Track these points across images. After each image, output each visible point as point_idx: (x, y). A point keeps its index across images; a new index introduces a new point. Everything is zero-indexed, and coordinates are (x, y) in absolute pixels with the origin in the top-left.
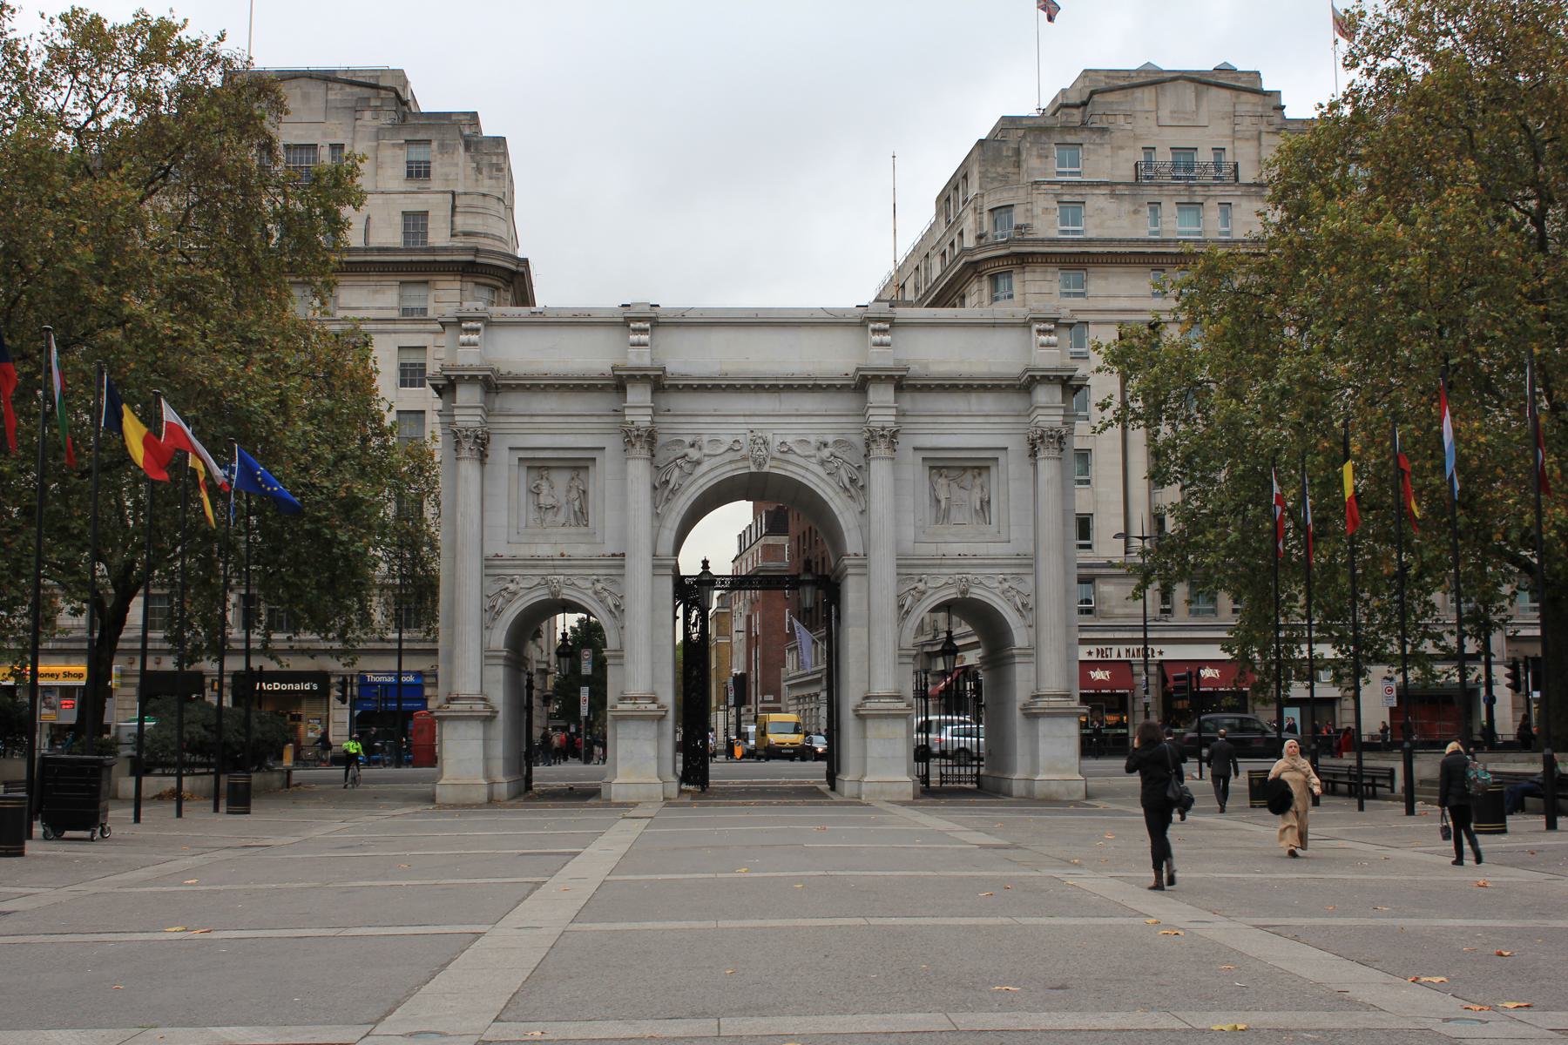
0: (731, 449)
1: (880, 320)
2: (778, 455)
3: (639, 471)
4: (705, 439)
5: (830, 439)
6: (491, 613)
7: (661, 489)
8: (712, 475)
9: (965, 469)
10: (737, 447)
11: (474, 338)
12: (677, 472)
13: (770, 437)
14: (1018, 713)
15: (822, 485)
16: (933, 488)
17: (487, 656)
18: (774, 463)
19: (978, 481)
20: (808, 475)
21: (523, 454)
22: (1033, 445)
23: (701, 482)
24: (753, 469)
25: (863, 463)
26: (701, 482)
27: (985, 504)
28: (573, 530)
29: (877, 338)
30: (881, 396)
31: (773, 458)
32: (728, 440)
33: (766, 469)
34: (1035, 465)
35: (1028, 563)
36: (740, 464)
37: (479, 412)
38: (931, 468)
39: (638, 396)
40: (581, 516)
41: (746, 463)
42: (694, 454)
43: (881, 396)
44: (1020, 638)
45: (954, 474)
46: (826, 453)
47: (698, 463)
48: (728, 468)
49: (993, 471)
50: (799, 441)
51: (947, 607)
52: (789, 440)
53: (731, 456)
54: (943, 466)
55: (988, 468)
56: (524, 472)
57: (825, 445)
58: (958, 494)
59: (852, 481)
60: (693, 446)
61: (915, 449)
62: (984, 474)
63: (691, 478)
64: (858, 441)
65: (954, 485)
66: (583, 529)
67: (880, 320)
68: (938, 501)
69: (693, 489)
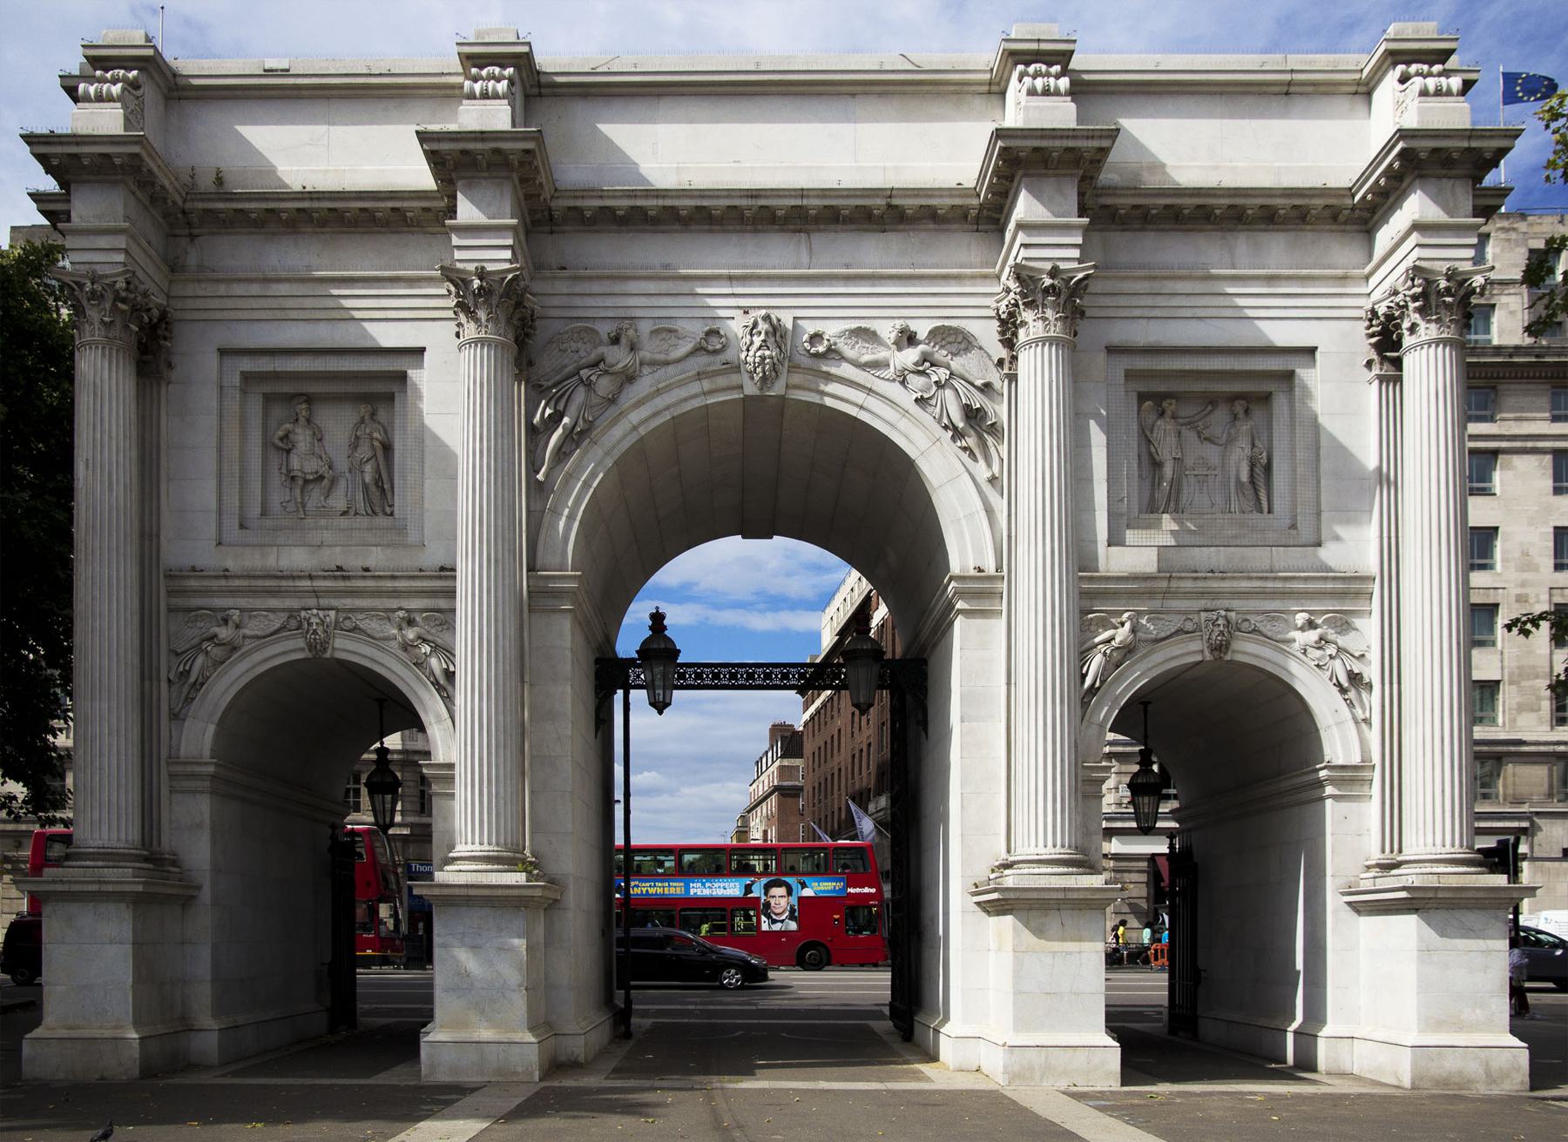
0: (699, 350)
2: (806, 362)
4: (645, 327)
5: (922, 329)
8: (660, 402)
9: (1212, 401)
10: (715, 344)
12: (580, 395)
13: (787, 320)
15: (903, 424)
16: (1146, 438)
18: (796, 379)
19: (1245, 427)
20: (872, 402)
23: (635, 417)
24: (751, 389)
25: (994, 377)
26: (635, 417)
27: (1262, 471)
28: (363, 521)
31: (794, 368)
32: (698, 329)
33: (777, 389)
36: (722, 381)
37: (121, 241)
38: (1142, 397)
40: (380, 494)
41: (734, 379)
42: (619, 357)
45: (1188, 410)
46: (911, 356)
47: (629, 378)
48: (695, 388)
49: (1280, 404)
52: (831, 330)
53: (701, 361)
55: (1266, 398)
57: (909, 338)
58: (1197, 451)
59: (973, 415)
60: (615, 341)
61: (1112, 350)
62: (1258, 413)
63: (612, 411)
65: (1190, 436)
66: (381, 521)
68: (1156, 465)
69: (617, 432)
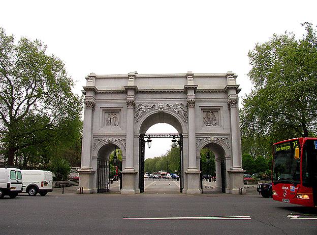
1: (191, 75)
3: (130, 112)
6: (93, 147)
7: (136, 115)
11: (91, 80)
14: (227, 173)
17: (92, 158)
21: (103, 109)
22: (229, 105)
29: (190, 79)
30: (191, 93)
34: (230, 110)
35: (230, 135)
39: (131, 93)
43: (191, 93)
44: (227, 154)
50: (172, 104)
51: (207, 146)
54: (206, 110)
56: (104, 112)
64: (185, 105)
67: (191, 75)
